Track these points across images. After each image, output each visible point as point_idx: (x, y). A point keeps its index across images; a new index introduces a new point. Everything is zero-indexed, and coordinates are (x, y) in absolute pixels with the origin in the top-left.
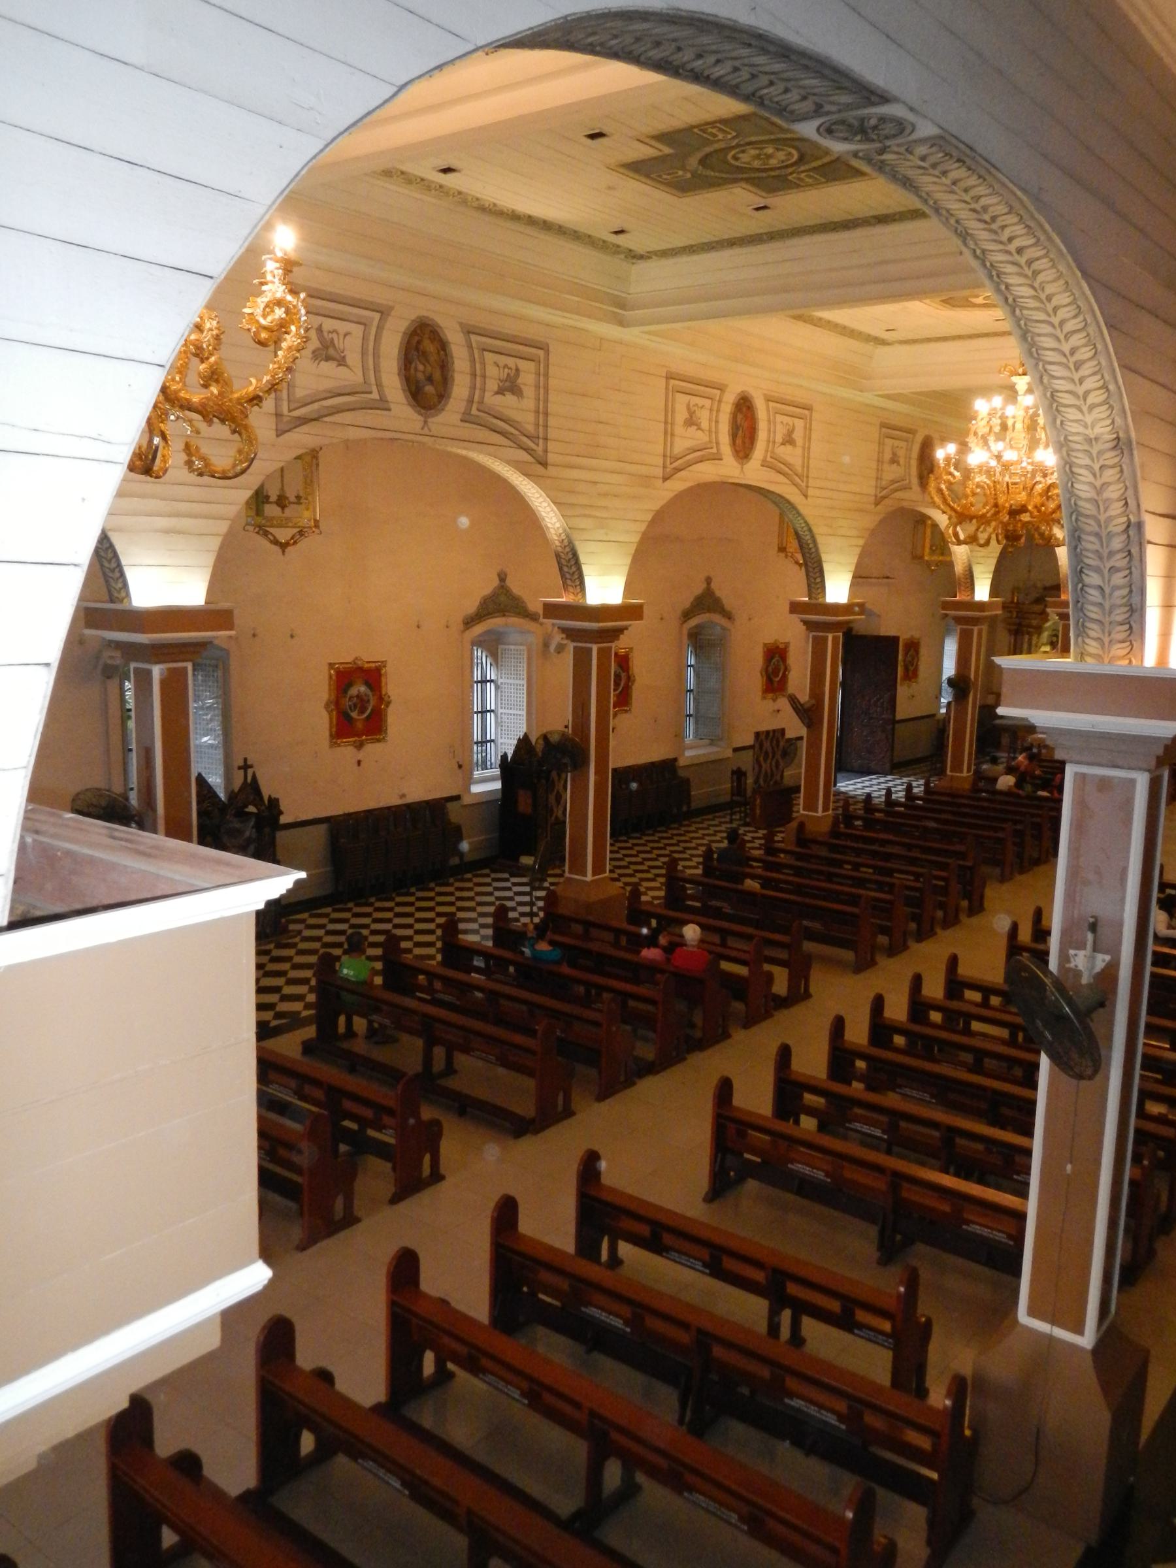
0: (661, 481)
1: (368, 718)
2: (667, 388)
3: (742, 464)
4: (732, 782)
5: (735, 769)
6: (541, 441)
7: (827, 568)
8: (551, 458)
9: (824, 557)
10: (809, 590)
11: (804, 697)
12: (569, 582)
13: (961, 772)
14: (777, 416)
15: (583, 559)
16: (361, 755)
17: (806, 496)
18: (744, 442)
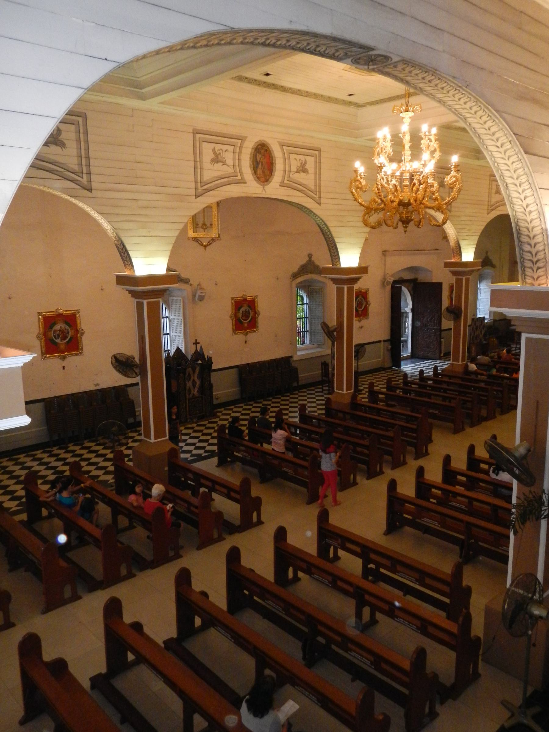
0: (194, 197)
1: (68, 342)
2: (194, 140)
3: (264, 186)
4: (322, 370)
5: (323, 361)
6: (85, 176)
7: (339, 246)
8: (94, 185)
9: (337, 240)
10: (332, 260)
11: (333, 322)
12: (126, 263)
13: (459, 362)
14: (291, 155)
15: (128, 248)
16: (64, 363)
17: (319, 204)
18: (263, 172)
